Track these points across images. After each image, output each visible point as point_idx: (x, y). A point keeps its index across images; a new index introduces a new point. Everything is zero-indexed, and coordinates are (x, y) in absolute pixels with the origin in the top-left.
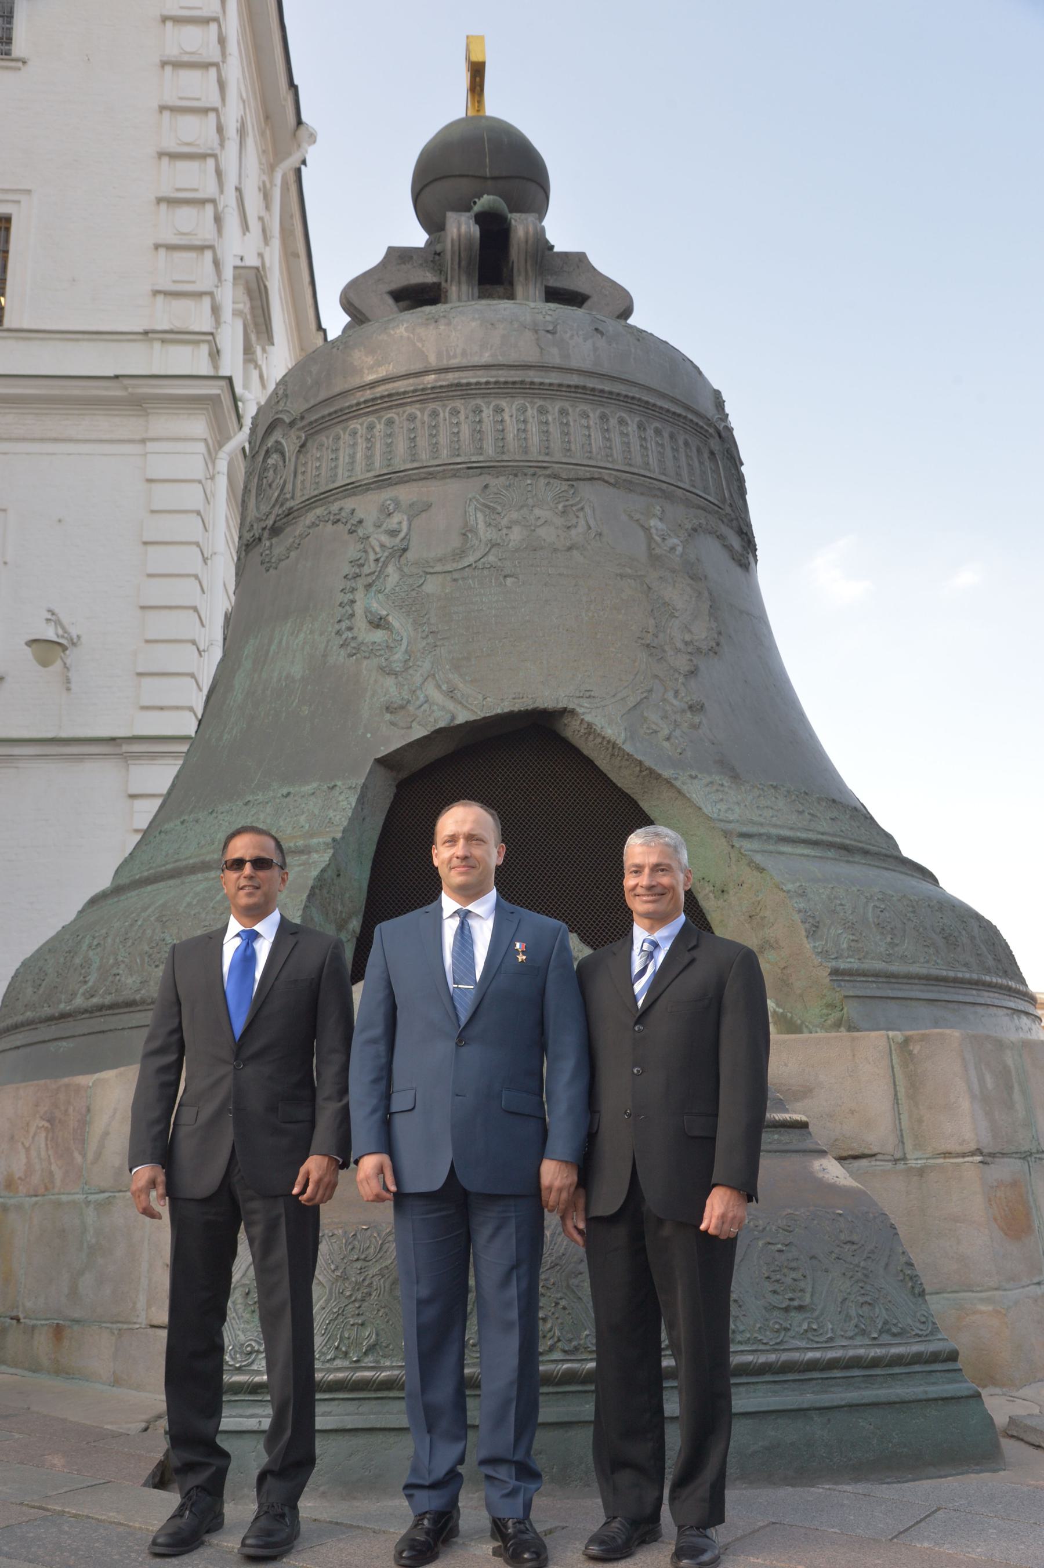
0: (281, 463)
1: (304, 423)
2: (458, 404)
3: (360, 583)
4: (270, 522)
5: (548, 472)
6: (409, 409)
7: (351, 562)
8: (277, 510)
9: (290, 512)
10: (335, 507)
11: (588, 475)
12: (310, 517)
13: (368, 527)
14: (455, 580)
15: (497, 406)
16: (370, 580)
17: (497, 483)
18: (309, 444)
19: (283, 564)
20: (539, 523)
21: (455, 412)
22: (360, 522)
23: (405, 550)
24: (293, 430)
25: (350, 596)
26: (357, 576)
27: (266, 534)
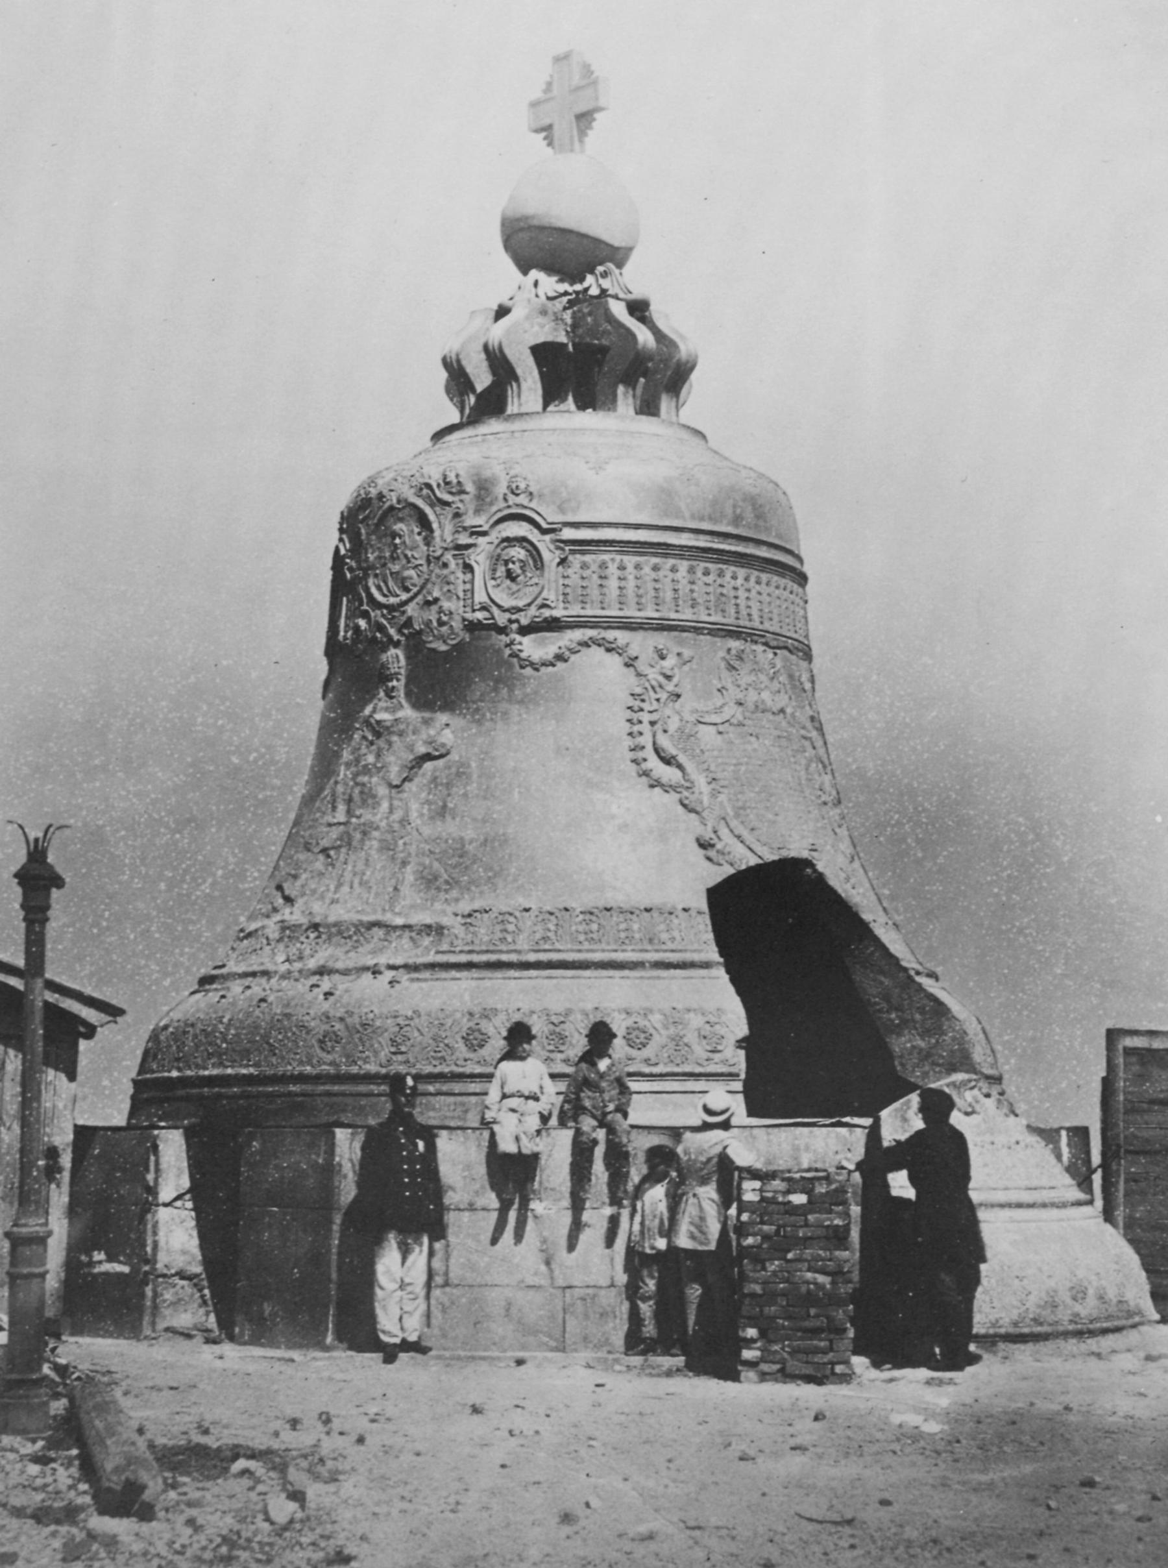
0: (531, 562)
1: (568, 534)
2: (710, 566)
3: (646, 717)
4: (525, 621)
5: (763, 640)
6: (671, 562)
7: (632, 695)
8: (533, 611)
9: (556, 620)
10: (610, 635)
11: (781, 644)
12: (578, 635)
13: (641, 665)
14: (720, 733)
15: (734, 573)
16: (654, 717)
17: (735, 644)
18: (571, 558)
19: (543, 669)
20: (763, 686)
21: (706, 573)
22: (636, 658)
23: (678, 696)
24: (547, 538)
25: (636, 728)
26: (642, 710)
27: (515, 626)
